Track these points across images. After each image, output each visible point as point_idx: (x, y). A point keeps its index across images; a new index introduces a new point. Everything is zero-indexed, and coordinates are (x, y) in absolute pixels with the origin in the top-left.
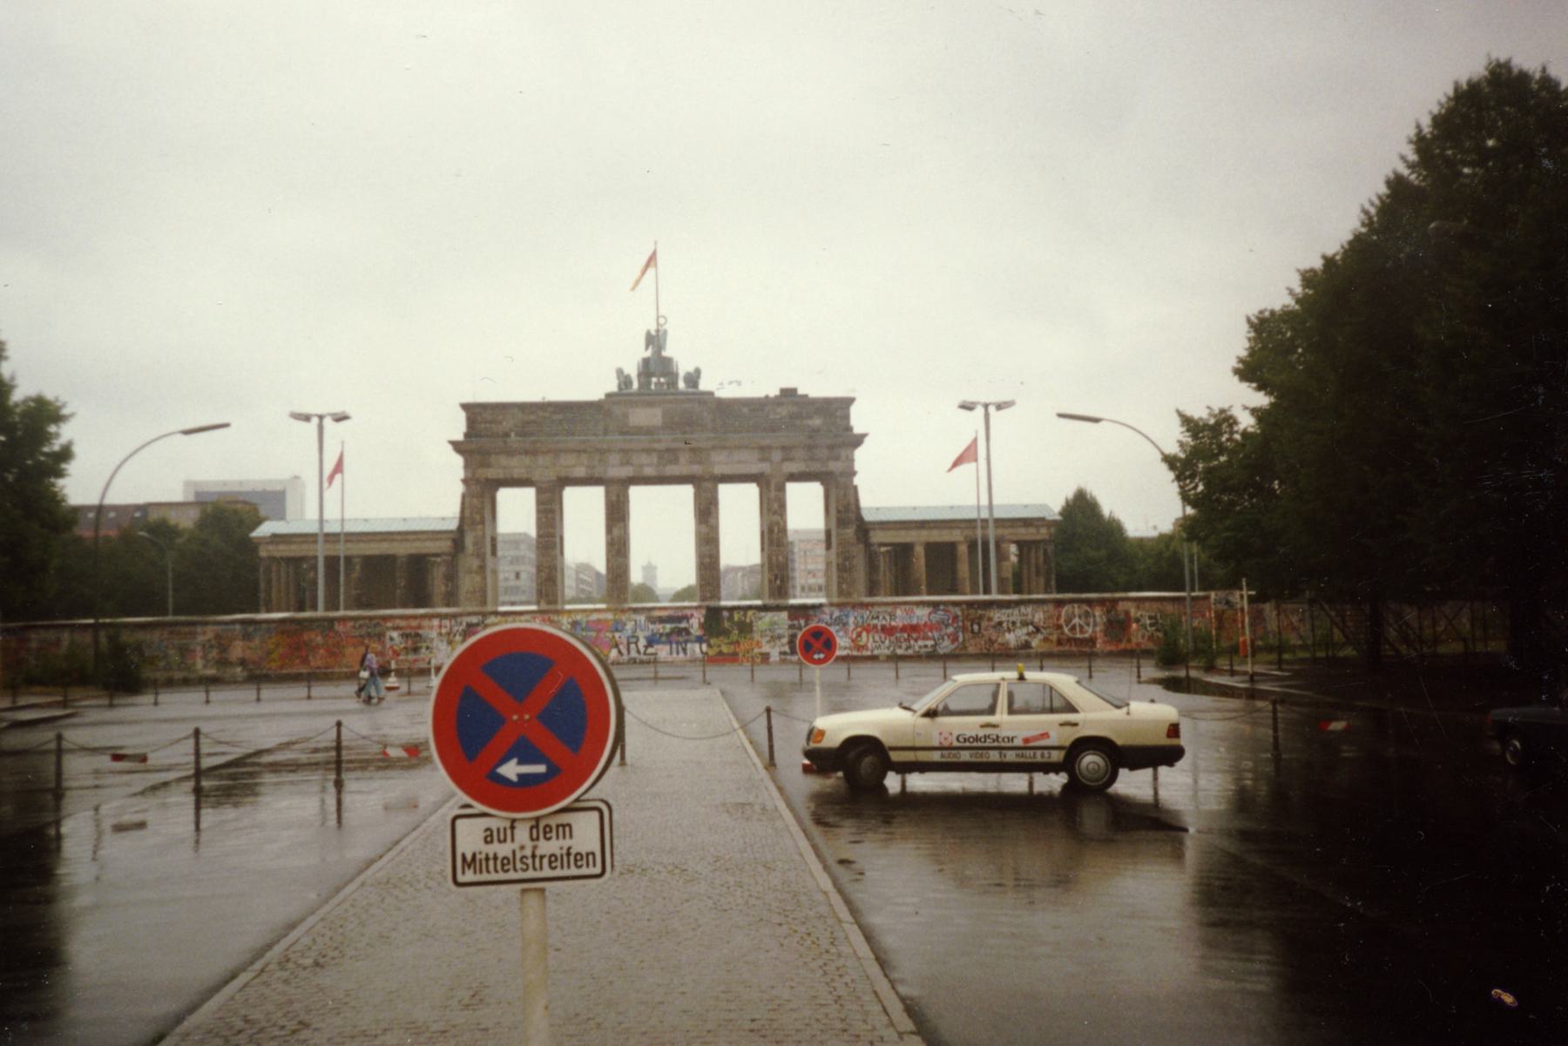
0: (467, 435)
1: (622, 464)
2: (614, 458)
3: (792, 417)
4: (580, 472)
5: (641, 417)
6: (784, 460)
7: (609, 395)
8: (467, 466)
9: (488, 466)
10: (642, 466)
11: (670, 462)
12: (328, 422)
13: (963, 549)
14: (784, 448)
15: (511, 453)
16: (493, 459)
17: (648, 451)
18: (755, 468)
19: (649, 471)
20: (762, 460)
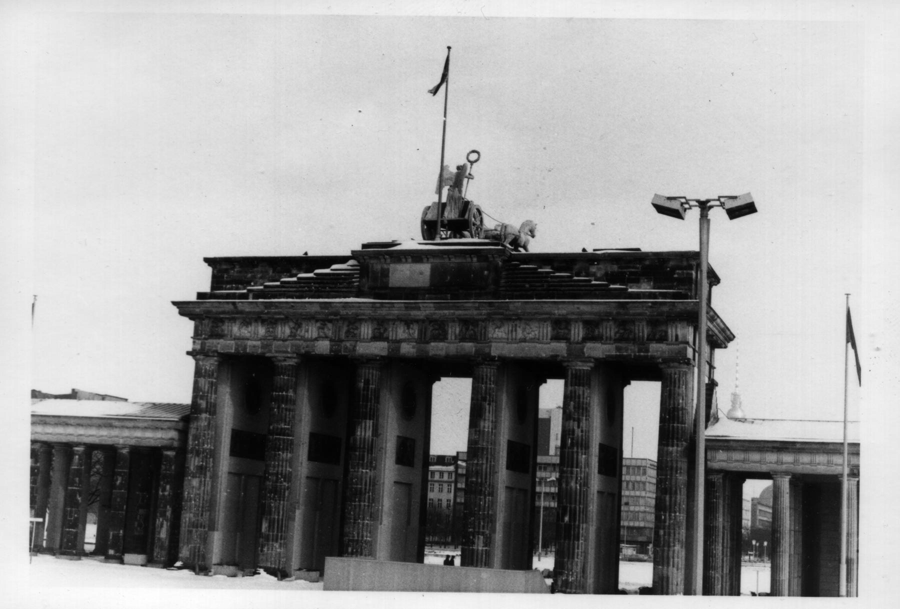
1: (376, 338)
2: (366, 330)
5: (402, 274)
6: (586, 339)
7: (364, 246)
8: (197, 335)
9: (220, 336)
10: (400, 341)
11: (436, 338)
14: (588, 324)
15: (247, 320)
16: (226, 327)
17: (408, 322)
19: (407, 349)
20: (556, 338)
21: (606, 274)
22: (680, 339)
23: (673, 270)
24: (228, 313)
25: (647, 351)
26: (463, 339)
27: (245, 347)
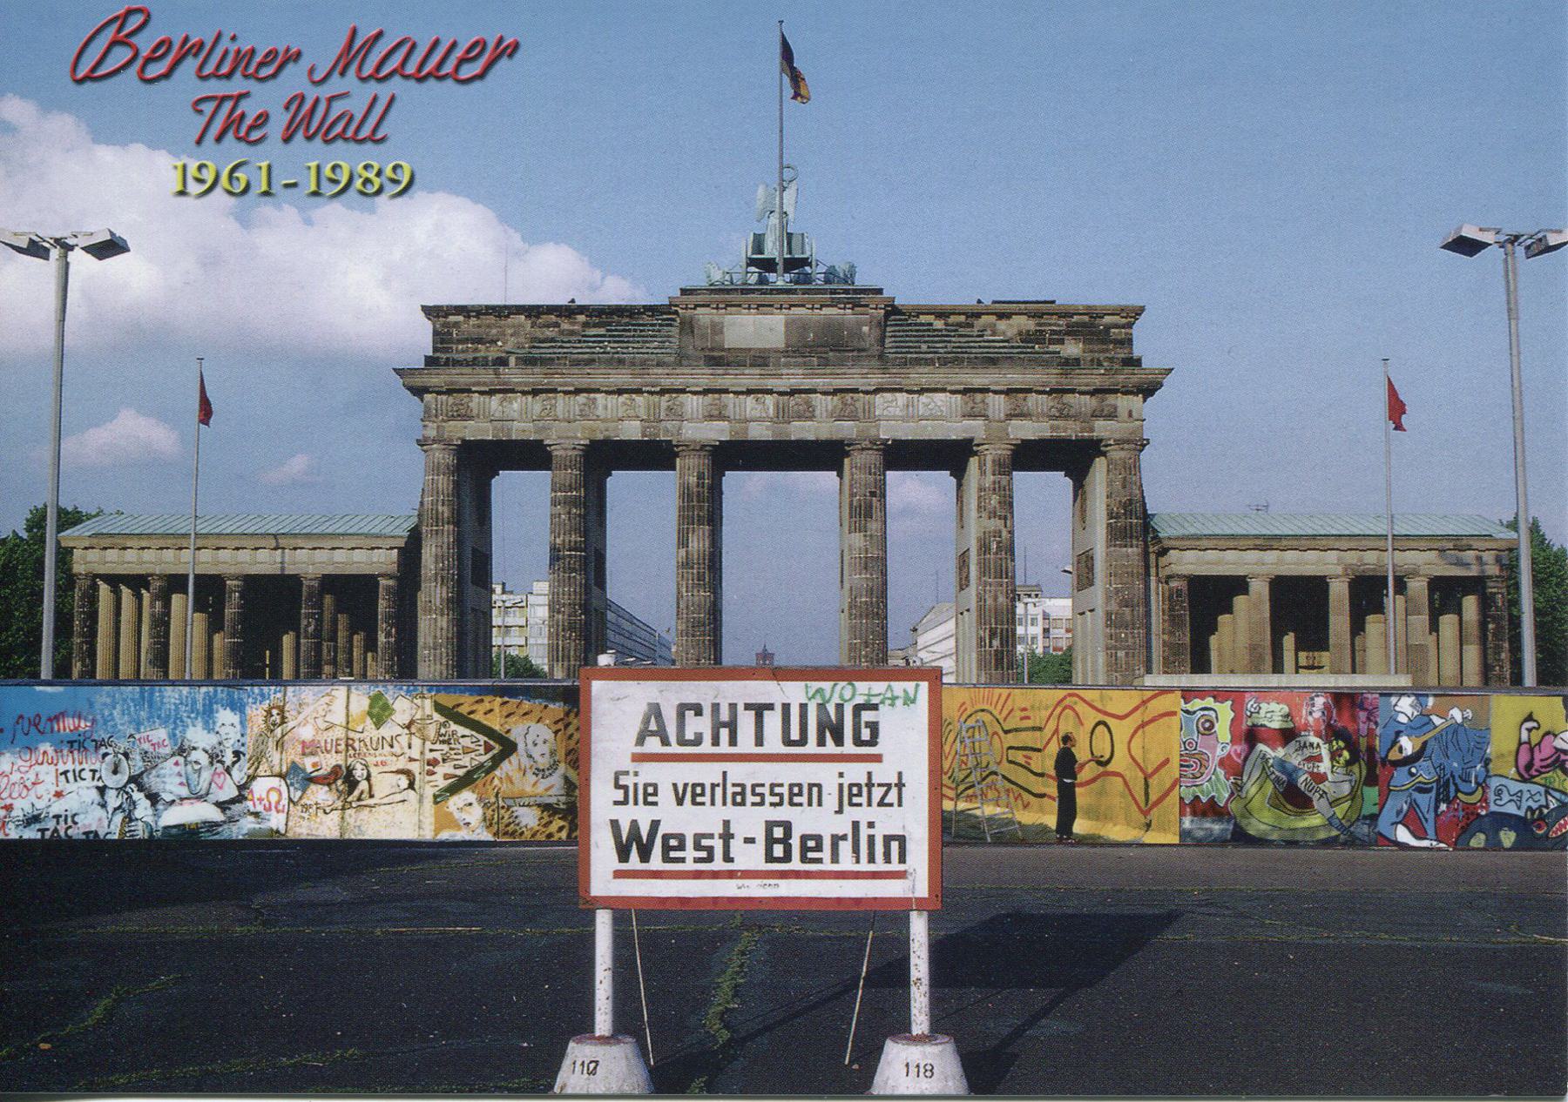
0: (430, 361)
3: (1027, 338)
4: (632, 431)
6: (1010, 416)
7: (684, 292)
12: (78, 258)
13: (1339, 591)
18: (955, 430)
19: (760, 432)
20: (971, 415)
21: (1020, 333)
22: (1135, 414)
23: (1108, 328)
24: (485, 384)
25: (1092, 430)
27: (510, 430)
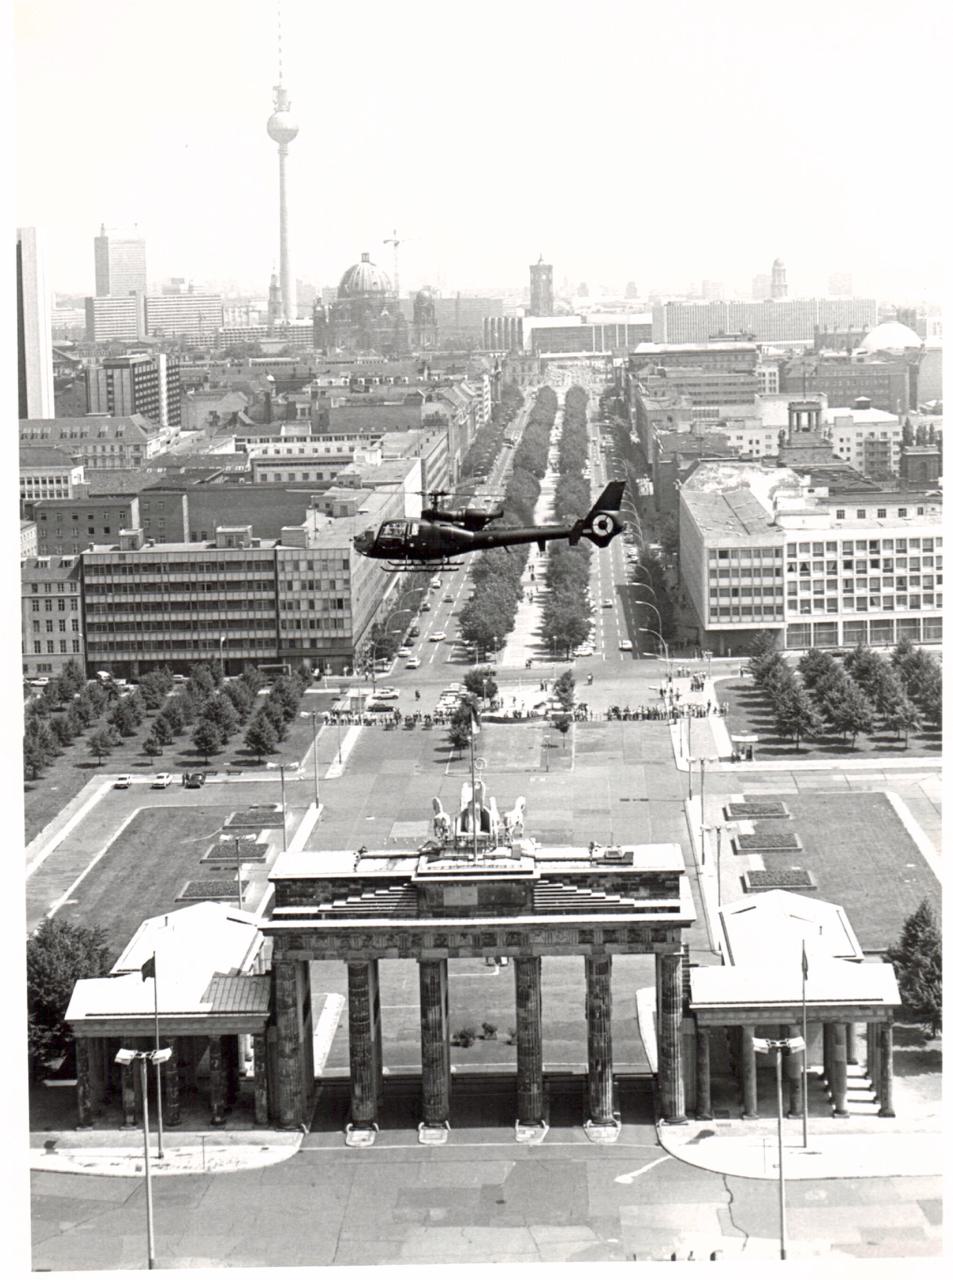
6: (605, 942)
9: (300, 948)
26: (509, 945)
